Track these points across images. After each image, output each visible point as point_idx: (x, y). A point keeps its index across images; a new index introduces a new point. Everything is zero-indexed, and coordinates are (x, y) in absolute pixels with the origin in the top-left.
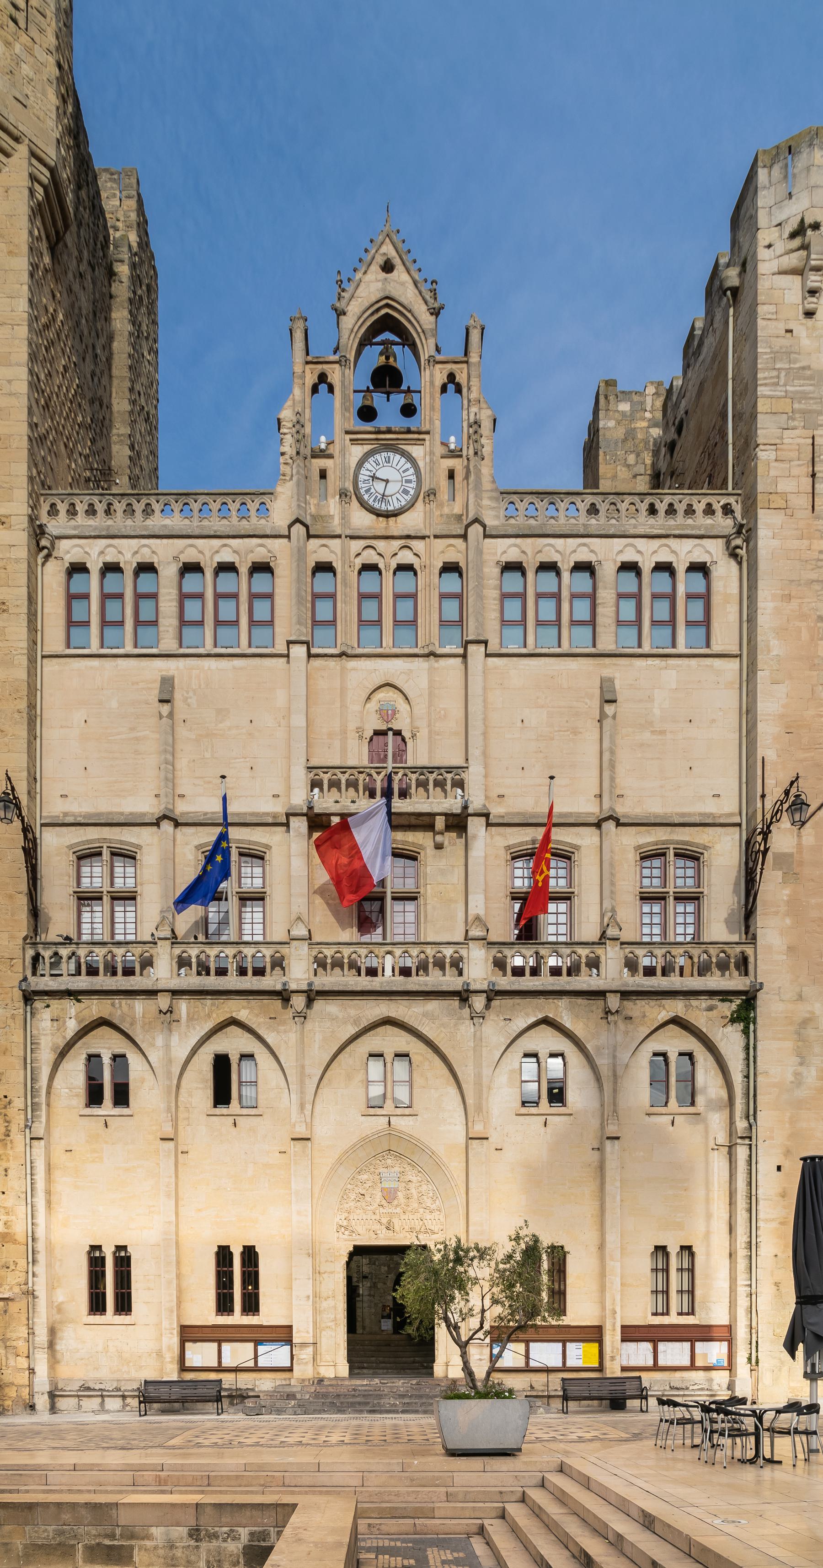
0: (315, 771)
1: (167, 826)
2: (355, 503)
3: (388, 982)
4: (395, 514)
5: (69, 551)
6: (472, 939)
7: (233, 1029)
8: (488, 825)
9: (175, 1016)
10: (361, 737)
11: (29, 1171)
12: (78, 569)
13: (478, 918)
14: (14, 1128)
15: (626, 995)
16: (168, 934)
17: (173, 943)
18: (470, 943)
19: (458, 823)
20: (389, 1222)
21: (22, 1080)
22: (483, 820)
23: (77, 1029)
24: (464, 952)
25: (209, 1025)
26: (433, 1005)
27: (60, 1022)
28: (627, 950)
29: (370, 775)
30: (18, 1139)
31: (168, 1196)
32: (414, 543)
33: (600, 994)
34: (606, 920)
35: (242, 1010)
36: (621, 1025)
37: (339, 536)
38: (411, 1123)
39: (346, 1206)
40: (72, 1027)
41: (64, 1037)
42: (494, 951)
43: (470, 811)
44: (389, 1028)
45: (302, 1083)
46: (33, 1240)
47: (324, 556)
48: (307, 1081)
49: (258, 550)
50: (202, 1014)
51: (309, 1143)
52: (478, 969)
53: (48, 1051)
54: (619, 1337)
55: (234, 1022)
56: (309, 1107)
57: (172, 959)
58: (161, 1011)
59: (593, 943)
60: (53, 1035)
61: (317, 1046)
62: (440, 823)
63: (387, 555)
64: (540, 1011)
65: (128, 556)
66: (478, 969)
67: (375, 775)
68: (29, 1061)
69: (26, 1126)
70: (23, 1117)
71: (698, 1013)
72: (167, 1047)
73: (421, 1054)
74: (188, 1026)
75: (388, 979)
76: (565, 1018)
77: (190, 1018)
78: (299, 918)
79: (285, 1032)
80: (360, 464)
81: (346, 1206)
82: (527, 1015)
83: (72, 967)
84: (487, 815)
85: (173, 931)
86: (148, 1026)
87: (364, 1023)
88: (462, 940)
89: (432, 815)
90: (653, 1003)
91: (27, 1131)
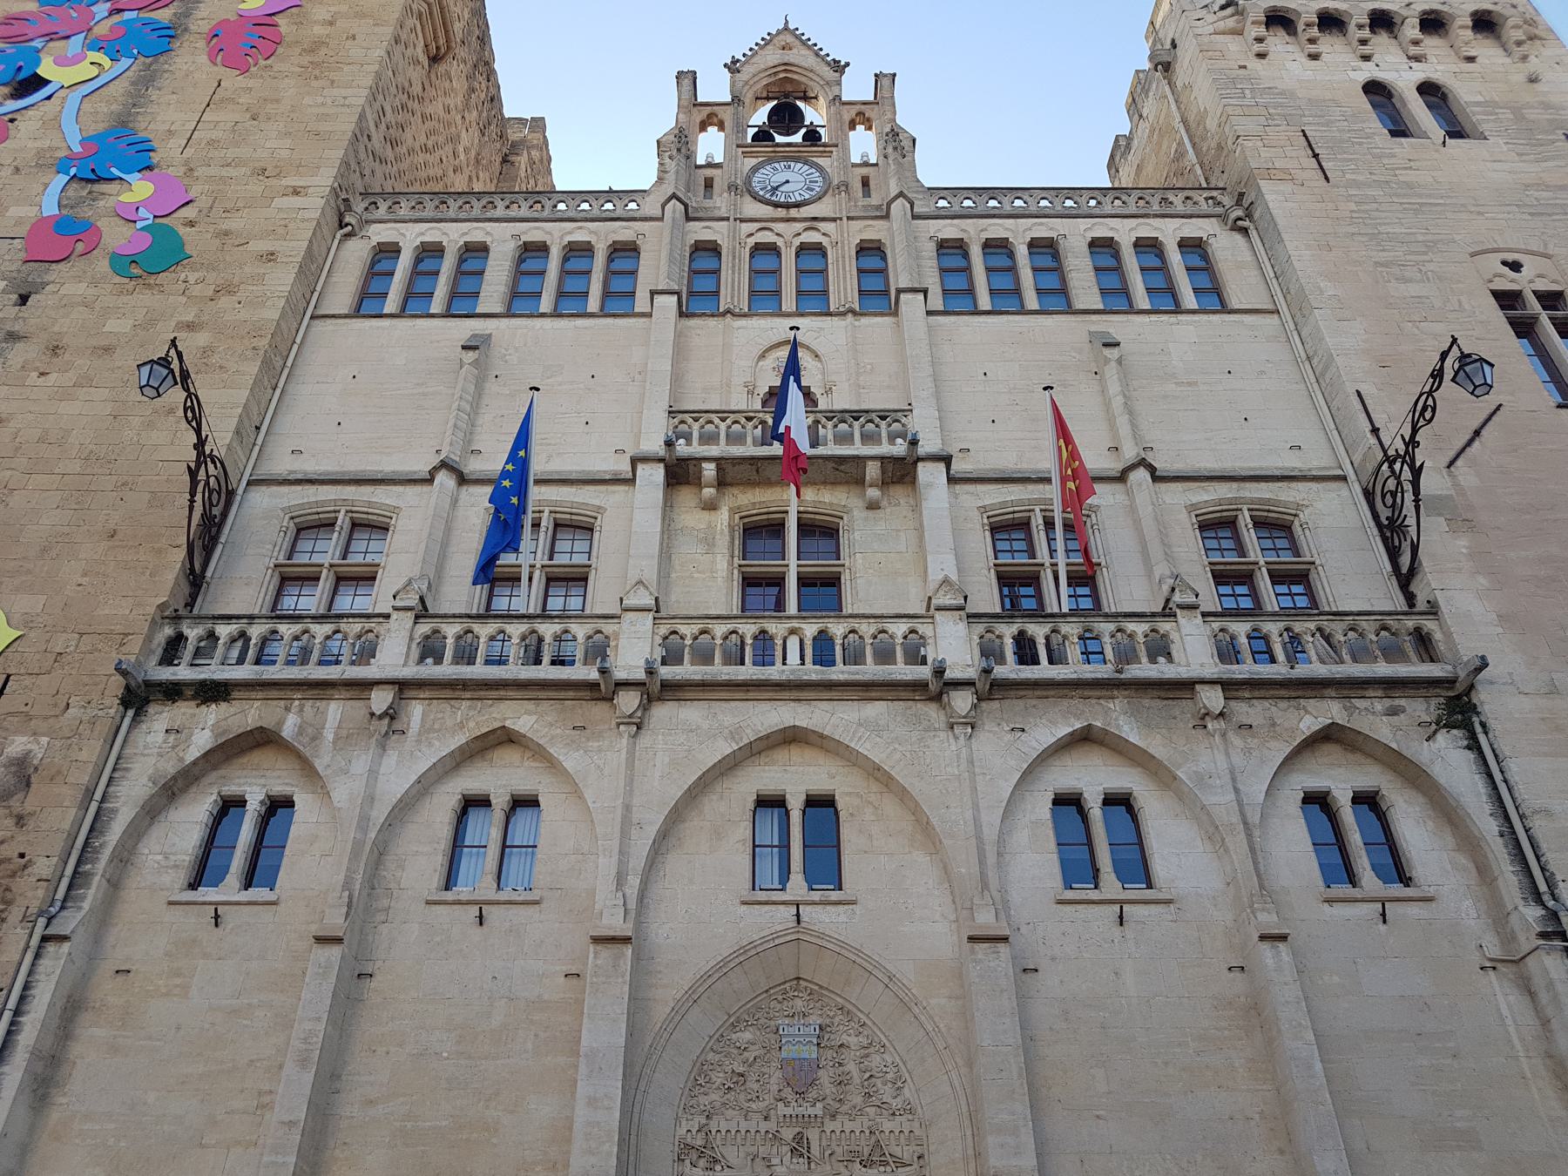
0: (680, 416)
1: (445, 480)
2: (748, 198)
3: (793, 671)
4: (797, 205)
5: (381, 233)
7: (509, 755)
8: (952, 480)
9: (397, 726)
10: (751, 393)
11: (12, 1004)
12: (389, 251)
15: (1230, 687)
16: (413, 601)
17: (417, 617)
18: (938, 615)
19: (901, 472)
20: (799, 1137)
21: (66, 825)
22: (942, 466)
24: (924, 629)
25: (460, 739)
26: (876, 710)
28: (1216, 626)
31: (303, 1063)
32: (821, 225)
33: (1185, 687)
34: (1166, 588)
35: (523, 718)
36: (1236, 740)
37: (728, 219)
38: (843, 918)
40: (201, 741)
41: (181, 760)
42: (980, 628)
43: (922, 449)
44: (796, 753)
45: (624, 834)
47: (706, 235)
48: (634, 832)
49: (624, 232)
50: (449, 723)
51: (628, 951)
52: (954, 647)
53: (145, 780)
55: (505, 738)
56: (634, 882)
57: (411, 639)
58: (372, 714)
59: (1153, 615)
61: (657, 774)
62: (873, 471)
63: (788, 237)
65: (454, 236)
66: (954, 647)
68: (98, 796)
69: (40, 914)
70: (40, 893)
71: (1372, 719)
72: (373, 773)
74: (419, 741)
75: (793, 664)
76: (1126, 728)
77: (425, 730)
78: (640, 582)
79: (600, 750)
80: (755, 169)
81: (703, 1100)
82: (1054, 723)
83: (235, 653)
84: (947, 460)
85: (422, 599)
86: (344, 740)
87: (749, 736)
88: (923, 612)
89: (860, 460)
90: (1283, 704)
91: (42, 921)
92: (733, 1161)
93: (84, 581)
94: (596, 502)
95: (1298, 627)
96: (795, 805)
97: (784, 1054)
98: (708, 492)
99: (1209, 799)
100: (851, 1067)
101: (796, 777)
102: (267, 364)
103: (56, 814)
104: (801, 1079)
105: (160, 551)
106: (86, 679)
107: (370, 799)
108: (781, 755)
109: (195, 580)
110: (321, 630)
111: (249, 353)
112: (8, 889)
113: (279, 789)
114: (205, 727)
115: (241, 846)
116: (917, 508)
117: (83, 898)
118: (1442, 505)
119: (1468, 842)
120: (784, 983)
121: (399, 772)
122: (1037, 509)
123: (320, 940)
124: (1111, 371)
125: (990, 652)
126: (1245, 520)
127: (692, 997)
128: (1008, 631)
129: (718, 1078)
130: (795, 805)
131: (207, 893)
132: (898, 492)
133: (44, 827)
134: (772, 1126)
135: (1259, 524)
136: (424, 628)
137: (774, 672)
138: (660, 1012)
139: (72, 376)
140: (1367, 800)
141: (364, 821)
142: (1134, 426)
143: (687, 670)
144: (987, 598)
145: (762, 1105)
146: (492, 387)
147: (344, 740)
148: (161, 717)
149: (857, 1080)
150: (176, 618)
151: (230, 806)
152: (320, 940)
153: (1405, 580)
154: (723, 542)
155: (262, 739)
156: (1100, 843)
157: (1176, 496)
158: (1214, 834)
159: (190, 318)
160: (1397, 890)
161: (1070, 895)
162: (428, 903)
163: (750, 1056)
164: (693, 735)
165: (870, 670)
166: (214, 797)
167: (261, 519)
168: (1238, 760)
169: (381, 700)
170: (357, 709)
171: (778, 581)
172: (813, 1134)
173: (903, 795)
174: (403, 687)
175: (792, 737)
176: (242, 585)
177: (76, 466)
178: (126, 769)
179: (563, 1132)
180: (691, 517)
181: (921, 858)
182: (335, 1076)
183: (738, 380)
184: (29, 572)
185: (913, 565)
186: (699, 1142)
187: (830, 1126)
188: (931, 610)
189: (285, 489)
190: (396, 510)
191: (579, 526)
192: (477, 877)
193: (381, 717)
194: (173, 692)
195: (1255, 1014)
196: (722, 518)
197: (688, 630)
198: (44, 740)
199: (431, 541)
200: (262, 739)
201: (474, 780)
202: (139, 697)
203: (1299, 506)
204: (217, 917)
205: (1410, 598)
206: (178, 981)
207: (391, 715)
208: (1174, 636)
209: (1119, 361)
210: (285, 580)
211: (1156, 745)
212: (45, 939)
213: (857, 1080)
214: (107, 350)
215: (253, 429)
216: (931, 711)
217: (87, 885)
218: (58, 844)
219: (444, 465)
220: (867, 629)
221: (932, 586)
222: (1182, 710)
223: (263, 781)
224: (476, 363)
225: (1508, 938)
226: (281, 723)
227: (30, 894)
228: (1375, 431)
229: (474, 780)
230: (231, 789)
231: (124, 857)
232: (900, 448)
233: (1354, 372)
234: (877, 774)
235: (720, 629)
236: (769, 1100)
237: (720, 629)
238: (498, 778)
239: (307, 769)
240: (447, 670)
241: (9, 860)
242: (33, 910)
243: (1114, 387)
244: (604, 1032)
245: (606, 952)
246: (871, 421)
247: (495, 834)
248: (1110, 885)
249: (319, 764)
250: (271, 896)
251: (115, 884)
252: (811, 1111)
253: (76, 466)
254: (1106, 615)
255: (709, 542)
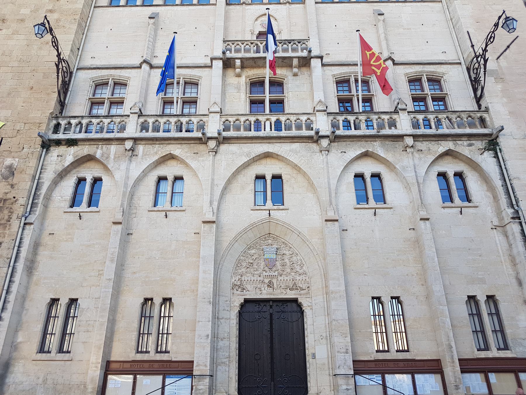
0: (227, 43)
1: (145, 66)
3: (268, 133)
6: (317, 111)
8: (323, 65)
9: (135, 153)
10: (252, 34)
11: (17, 244)
13: (320, 101)
14: (14, 216)
15: (415, 137)
16: (137, 110)
17: (139, 116)
18: (317, 113)
19: (305, 62)
20: (270, 282)
22: (320, 60)
23: (72, 161)
24: (312, 118)
25: (156, 158)
27: (63, 157)
28: (412, 116)
29: (257, 45)
30: (15, 224)
31: (112, 261)
33: (401, 137)
34: (396, 103)
35: (176, 150)
36: (416, 155)
39: (240, 271)
40: (69, 160)
41: (63, 166)
42: (331, 118)
43: (313, 54)
44: (269, 161)
46: (7, 293)
48: (215, 188)
51: (214, 225)
53: (52, 172)
54: (458, 368)
55: (171, 157)
56: (216, 204)
57: (137, 124)
58: (126, 150)
59: (391, 112)
60: (56, 164)
62: (295, 62)
64: (363, 148)
66: (323, 124)
67: (259, 44)
69: (23, 216)
70: (22, 209)
71: (463, 148)
72: (128, 169)
73: (289, 174)
74: (142, 159)
75: (267, 131)
76: (380, 151)
77: (144, 155)
78: (215, 103)
81: (239, 271)
83: (78, 129)
84: (321, 58)
86: (117, 158)
88: (312, 112)
89: (291, 58)
90: (433, 143)
91: (23, 218)
92: (249, 289)
93: (23, 105)
94: (199, 75)
95: (440, 116)
96: (269, 178)
97: (265, 257)
98: (238, 70)
99: (406, 175)
100: (287, 260)
101: (269, 169)
102: (79, 25)
103: (24, 185)
104: (271, 265)
105: (48, 94)
106: (29, 139)
107: (127, 178)
108: (264, 161)
109: (62, 104)
110: (106, 121)
111: (73, 21)
112: (11, 208)
113: (97, 175)
114: (70, 154)
115: (86, 194)
116: (310, 75)
117: (36, 211)
118: (494, 73)
119: (491, 188)
120: (265, 236)
121: (136, 168)
122: (352, 75)
123: (114, 223)
124: (381, 25)
125: (335, 126)
126: (424, 79)
127: (236, 239)
128: (341, 118)
129: (244, 264)
130: (269, 178)
131: (75, 209)
132: (304, 69)
133: (20, 188)
134: (261, 278)
135: (429, 80)
136: (142, 120)
137: (261, 134)
138: (225, 245)
139: (10, 32)
140: (459, 175)
141: (126, 185)
142: (388, 45)
143: (232, 133)
144: (334, 107)
145: (258, 272)
146: (160, 32)
147: (117, 158)
148: (55, 151)
149: (288, 265)
150: (57, 118)
151: (81, 181)
152: (114, 223)
153: (478, 100)
154: (243, 88)
155: (90, 158)
156: (369, 189)
157: (402, 71)
158: (407, 186)
159: (50, 8)
160: (466, 204)
161: (359, 206)
162: (149, 211)
163: (254, 257)
164: (234, 155)
165: (294, 132)
166: (75, 178)
167: (82, 84)
168: (417, 161)
169: (129, 144)
170: (121, 148)
171: (262, 102)
172: (274, 281)
173: (304, 174)
174: (135, 140)
175: (267, 155)
176: (78, 105)
177: (16, 64)
178: (45, 169)
179: (196, 282)
180: (232, 79)
181: (310, 195)
182: (122, 265)
183: (248, 29)
184: (4, 102)
185: (309, 95)
186: (239, 283)
187: (280, 278)
188: (315, 111)
189: (90, 71)
190: (129, 78)
191: (193, 83)
192: (164, 202)
193: (129, 151)
194: (58, 143)
195: (417, 243)
196: (243, 80)
197: (232, 119)
198: (17, 159)
199: (141, 90)
200: (90, 158)
201: (162, 171)
202: (47, 145)
203: (443, 74)
204: (80, 216)
205: (479, 106)
206: (70, 237)
207: (132, 150)
208: (398, 120)
209: (384, 21)
210: (93, 104)
211: (389, 157)
212: (25, 224)
213: (288, 265)
214: (22, 20)
215: (77, 49)
216: (314, 146)
217: (37, 207)
218: (26, 194)
219: (145, 61)
220: (293, 118)
221: (315, 103)
222: (399, 145)
223: (91, 172)
224: (154, 24)
225: (501, 219)
226: (95, 153)
227: (19, 210)
228: (473, 46)
229: (162, 171)
230: (81, 175)
231: (48, 197)
232: (305, 54)
233: (467, 24)
234: (296, 167)
235: (243, 119)
236: (260, 271)
237: (243, 119)
238: (169, 170)
239: (106, 168)
240: (150, 134)
241: (10, 199)
242: (20, 215)
243: (381, 30)
244: (208, 250)
245: (207, 226)
246: (295, 44)
247: (169, 189)
248: (372, 202)
249: (109, 167)
250: (97, 210)
251: (46, 207)
252: (274, 274)
253: (16, 64)
254: (375, 113)
255: (238, 89)
